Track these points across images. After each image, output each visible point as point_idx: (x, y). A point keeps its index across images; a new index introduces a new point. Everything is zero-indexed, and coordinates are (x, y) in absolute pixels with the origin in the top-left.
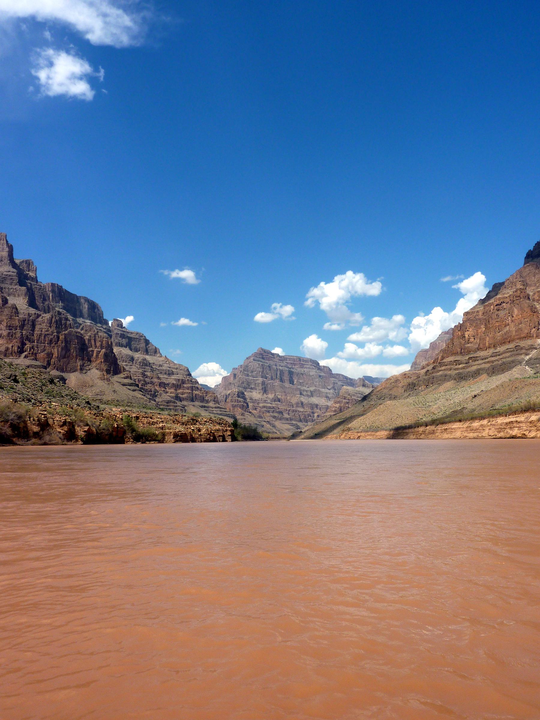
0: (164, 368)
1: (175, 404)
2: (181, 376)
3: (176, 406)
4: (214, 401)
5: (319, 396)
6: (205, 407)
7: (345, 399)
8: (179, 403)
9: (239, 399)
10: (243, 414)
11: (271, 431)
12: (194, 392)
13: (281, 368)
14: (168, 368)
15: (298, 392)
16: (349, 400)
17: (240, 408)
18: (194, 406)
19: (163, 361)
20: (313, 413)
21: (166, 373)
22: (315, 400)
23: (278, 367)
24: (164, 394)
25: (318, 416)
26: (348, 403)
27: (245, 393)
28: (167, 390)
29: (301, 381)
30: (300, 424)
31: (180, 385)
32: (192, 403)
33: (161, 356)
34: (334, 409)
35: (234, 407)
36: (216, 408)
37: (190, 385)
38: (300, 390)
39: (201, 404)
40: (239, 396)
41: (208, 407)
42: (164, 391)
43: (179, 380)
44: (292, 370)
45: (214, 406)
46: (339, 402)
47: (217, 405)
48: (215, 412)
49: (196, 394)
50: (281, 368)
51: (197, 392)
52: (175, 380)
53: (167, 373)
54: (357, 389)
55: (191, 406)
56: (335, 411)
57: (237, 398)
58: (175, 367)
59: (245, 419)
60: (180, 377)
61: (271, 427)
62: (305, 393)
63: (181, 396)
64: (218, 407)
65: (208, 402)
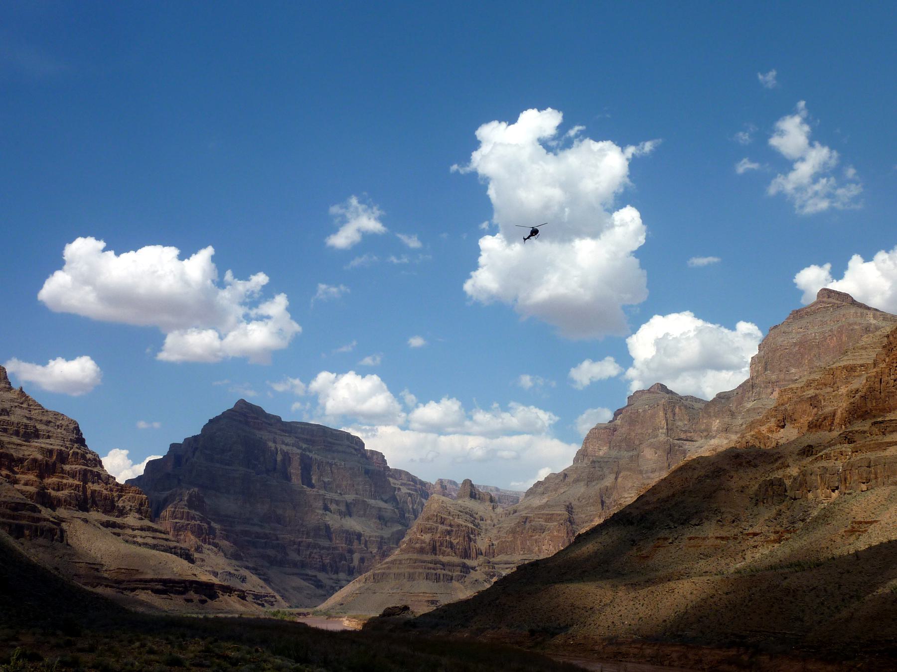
0: (13, 418)
1: (36, 515)
2: (58, 442)
3: (39, 520)
4: (139, 511)
5: (364, 515)
6: (114, 525)
7: (442, 523)
8: (46, 512)
9: (193, 512)
10: (198, 549)
11: (263, 592)
12: (90, 484)
13: (284, 448)
14: (25, 421)
15: (320, 504)
16: (451, 525)
17: (193, 533)
18: (86, 521)
19: (12, 400)
20: (351, 552)
21: (17, 433)
22: (353, 524)
23: (279, 446)
24: (8, 486)
25: (362, 560)
26: (449, 533)
27: (206, 500)
28: (18, 476)
29: (326, 480)
30: (321, 576)
31: (54, 464)
32: (80, 514)
33: (10, 389)
34: (418, 545)
35: (178, 529)
36: (142, 529)
37: (79, 467)
38: (324, 499)
39: (106, 518)
40: (190, 508)
41: (122, 527)
42: (7, 476)
43: (51, 452)
44: (308, 453)
45: (138, 524)
46: (430, 530)
47: (147, 523)
48: (139, 540)
49: (93, 492)
50: (284, 448)
51: (96, 487)
52: (42, 450)
53: (22, 431)
54: (460, 502)
55: (79, 522)
56: (422, 551)
57: (186, 510)
58: (45, 418)
59: (203, 560)
60: (55, 444)
61: (262, 583)
62: (333, 507)
63: (53, 493)
64: (149, 529)
65: (122, 513)
